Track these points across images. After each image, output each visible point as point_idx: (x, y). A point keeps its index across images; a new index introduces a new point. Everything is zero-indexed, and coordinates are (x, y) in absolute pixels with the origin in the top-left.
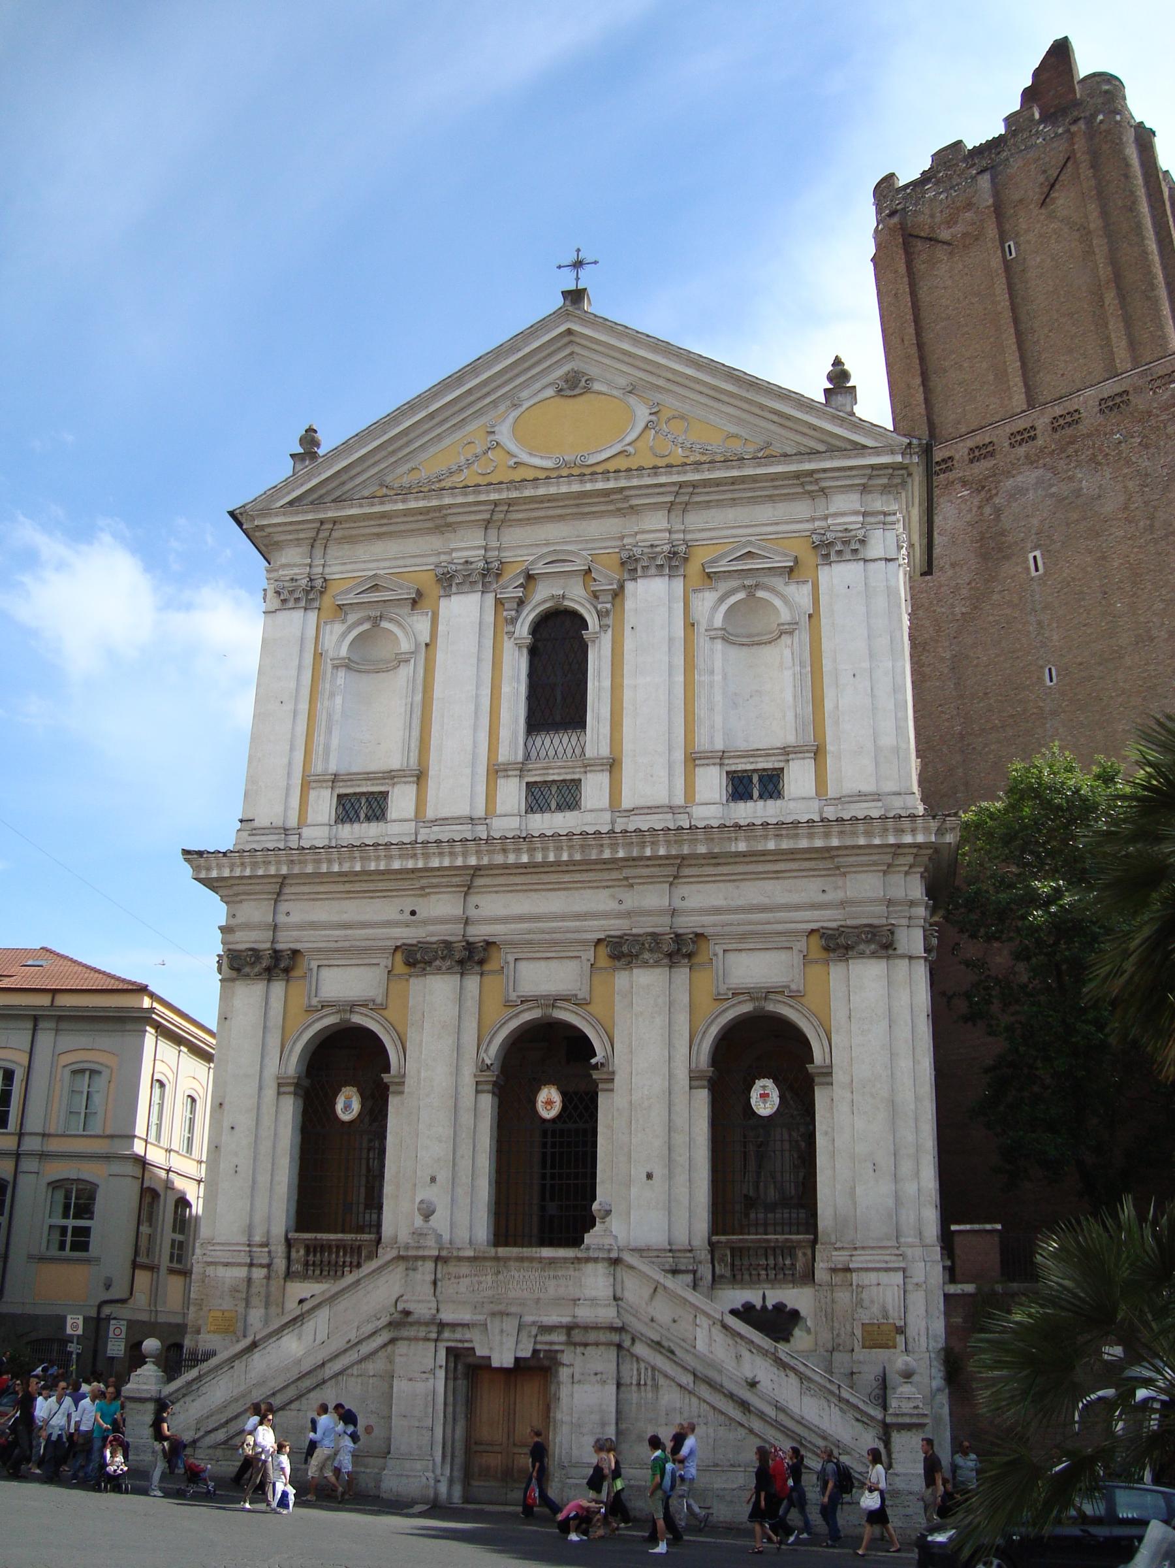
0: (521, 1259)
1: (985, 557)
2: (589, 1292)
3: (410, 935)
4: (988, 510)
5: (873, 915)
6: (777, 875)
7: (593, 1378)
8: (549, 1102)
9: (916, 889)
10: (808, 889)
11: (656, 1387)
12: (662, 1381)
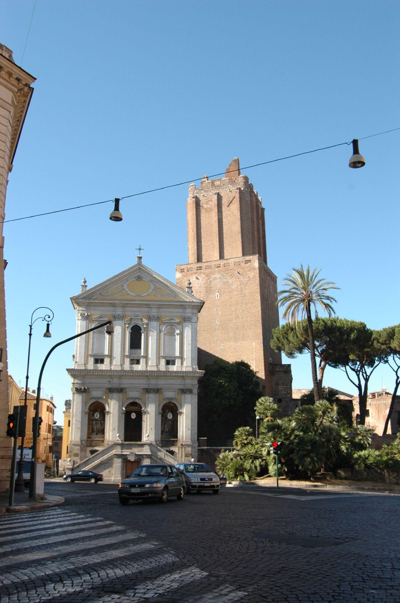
0: (135, 444)
1: (207, 292)
3: (109, 386)
4: (208, 281)
5: (189, 387)
6: (174, 379)
8: (133, 416)
9: (196, 382)
10: (179, 381)
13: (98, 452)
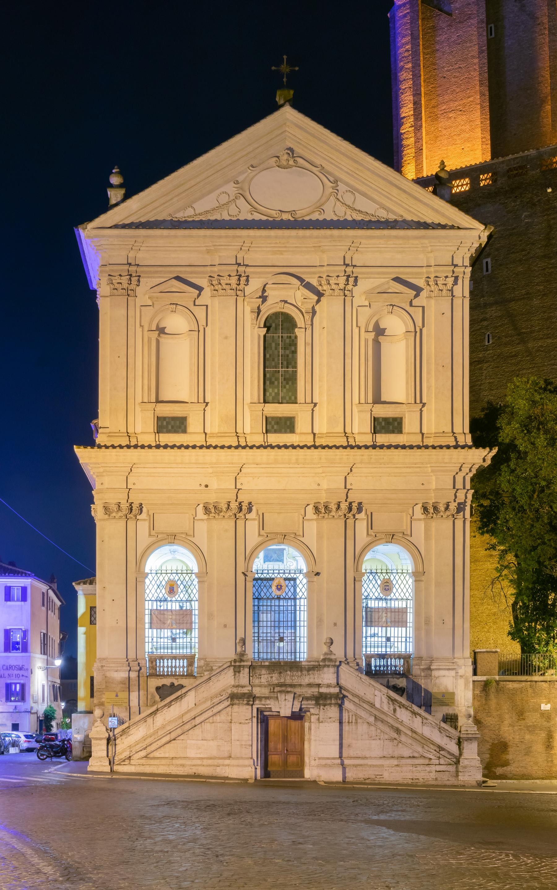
2: (326, 682)
7: (329, 720)
11: (356, 723)
12: (359, 721)
13: (184, 690)
